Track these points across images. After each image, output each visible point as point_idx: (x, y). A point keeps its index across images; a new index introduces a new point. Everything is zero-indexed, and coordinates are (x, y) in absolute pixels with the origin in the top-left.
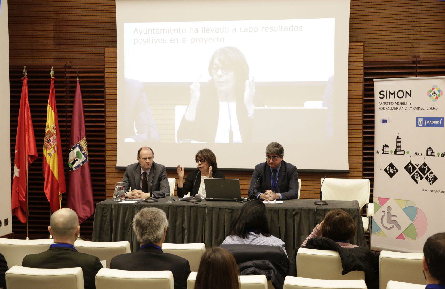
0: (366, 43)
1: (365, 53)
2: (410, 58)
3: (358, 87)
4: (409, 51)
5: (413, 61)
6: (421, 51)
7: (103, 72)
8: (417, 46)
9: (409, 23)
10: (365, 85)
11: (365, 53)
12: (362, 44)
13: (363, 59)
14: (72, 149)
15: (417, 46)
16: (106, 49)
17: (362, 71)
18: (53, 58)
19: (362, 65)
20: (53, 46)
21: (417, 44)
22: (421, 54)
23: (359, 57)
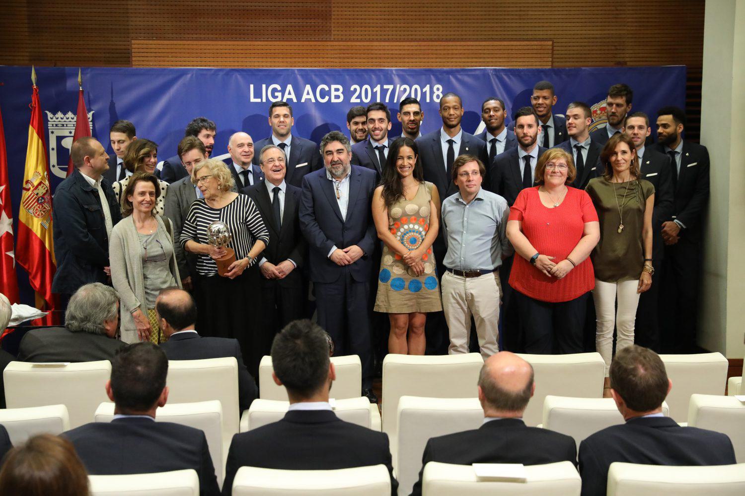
1: (555, 56)
4: (609, 56)
6: (627, 55)
8: (621, 47)
9: (610, 12)
11: (555, 56)
12: (550, 43)
13: (552, 66)
15: (621, 47)
16: (133, 41)
18: (27, 54)
20: (27, 34)
23: (545, 63)
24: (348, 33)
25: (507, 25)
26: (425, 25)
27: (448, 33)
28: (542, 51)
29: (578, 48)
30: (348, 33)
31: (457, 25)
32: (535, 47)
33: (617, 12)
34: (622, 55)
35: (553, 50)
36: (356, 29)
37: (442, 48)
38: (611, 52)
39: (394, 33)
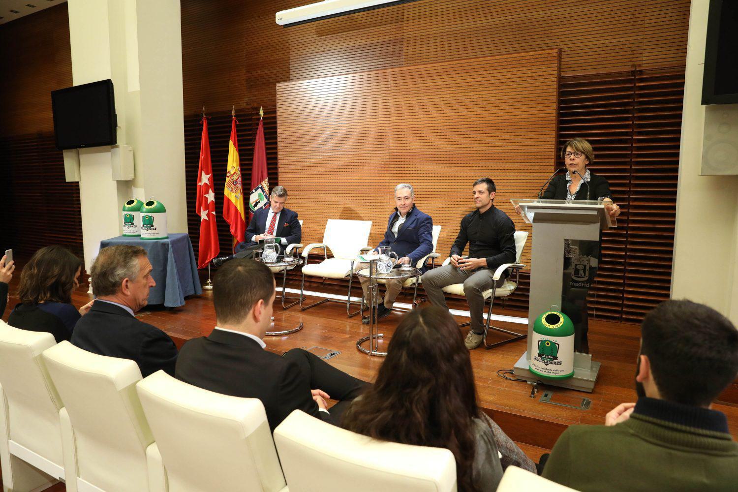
2: (628, 69)
3: (550, 108)
5: (632, 72)
6: (644, 58)
8: (639, 52)
14: (254, 191)
15: (639, 52)
21: (640, 48)
22: (644, 62)
28: (549, 59)
32: (543, 56)
33: (634, 20)
34: (639, 59)
37: (465, 65)
38: (629, 57)
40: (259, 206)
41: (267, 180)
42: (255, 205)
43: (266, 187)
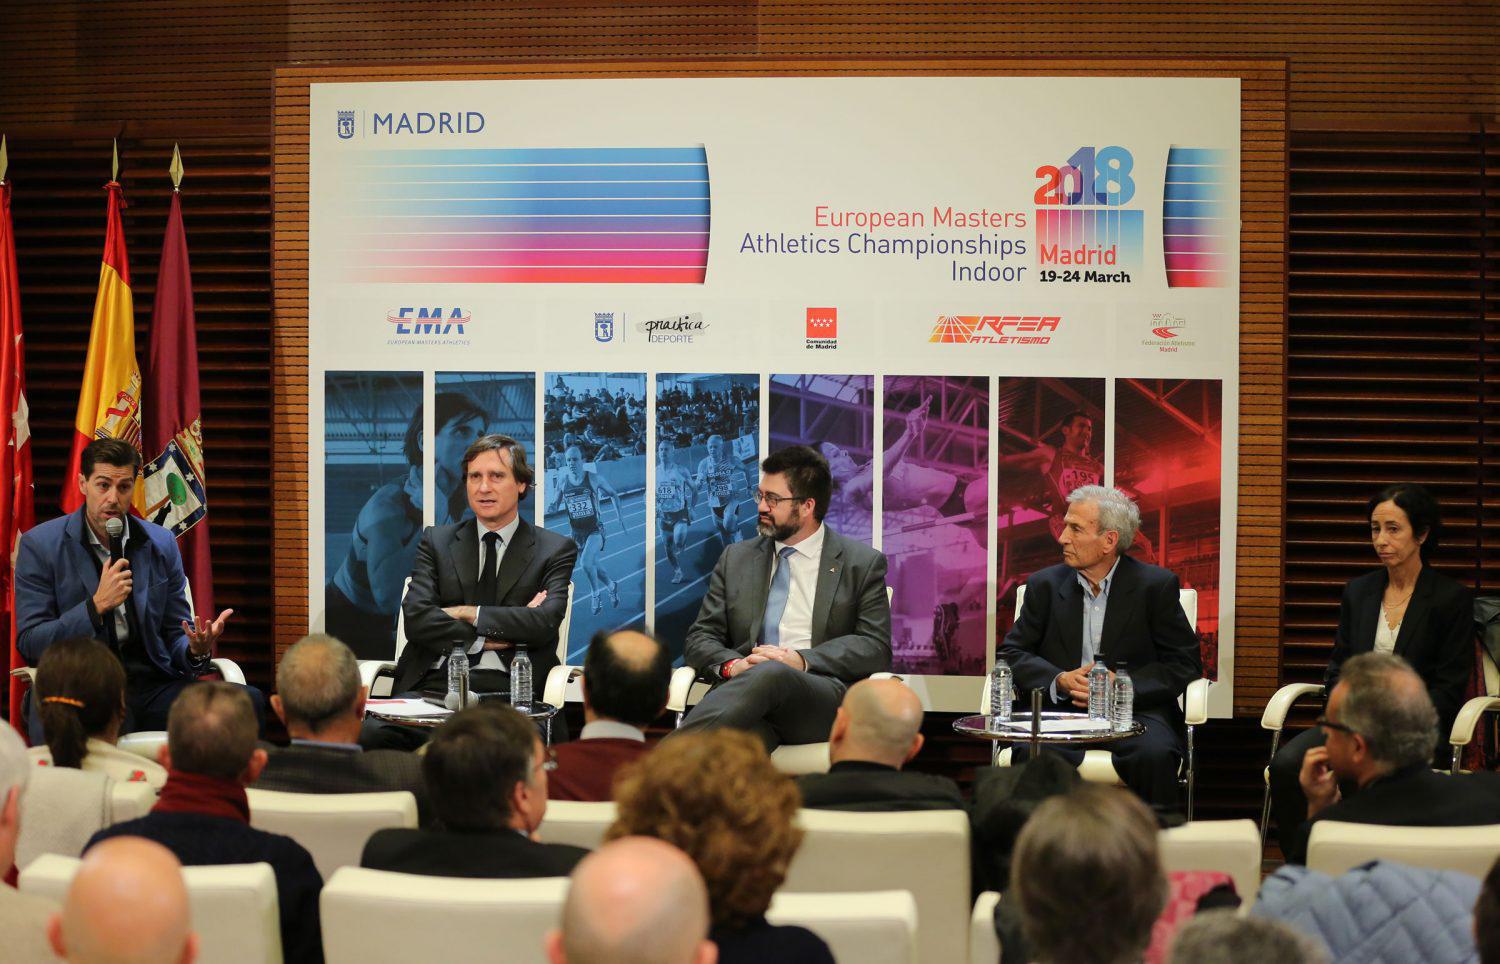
0: (1295, 58)
1: (1294, 96)
7: (266, 162)
8: (1485, 79)
10: (1294, 223)
12: (1282, 64)
13: (1287, 121)
15: (1485, 79)
16: (279, 72)
17: (1282, 166)
19: (1282, 144)
24: (797, 38)
25: (1194, 18)
26: (989, 18)
27: (1046, 37)
29: (1373, 78)
30: (797, 38)
31: (1067, 17)
35: (1288, 80)
36: (816, 28)
39: (912, 37)
40: (176, 517)
41: (197, 423)
42: (160, 520)
43: (197, 449)
